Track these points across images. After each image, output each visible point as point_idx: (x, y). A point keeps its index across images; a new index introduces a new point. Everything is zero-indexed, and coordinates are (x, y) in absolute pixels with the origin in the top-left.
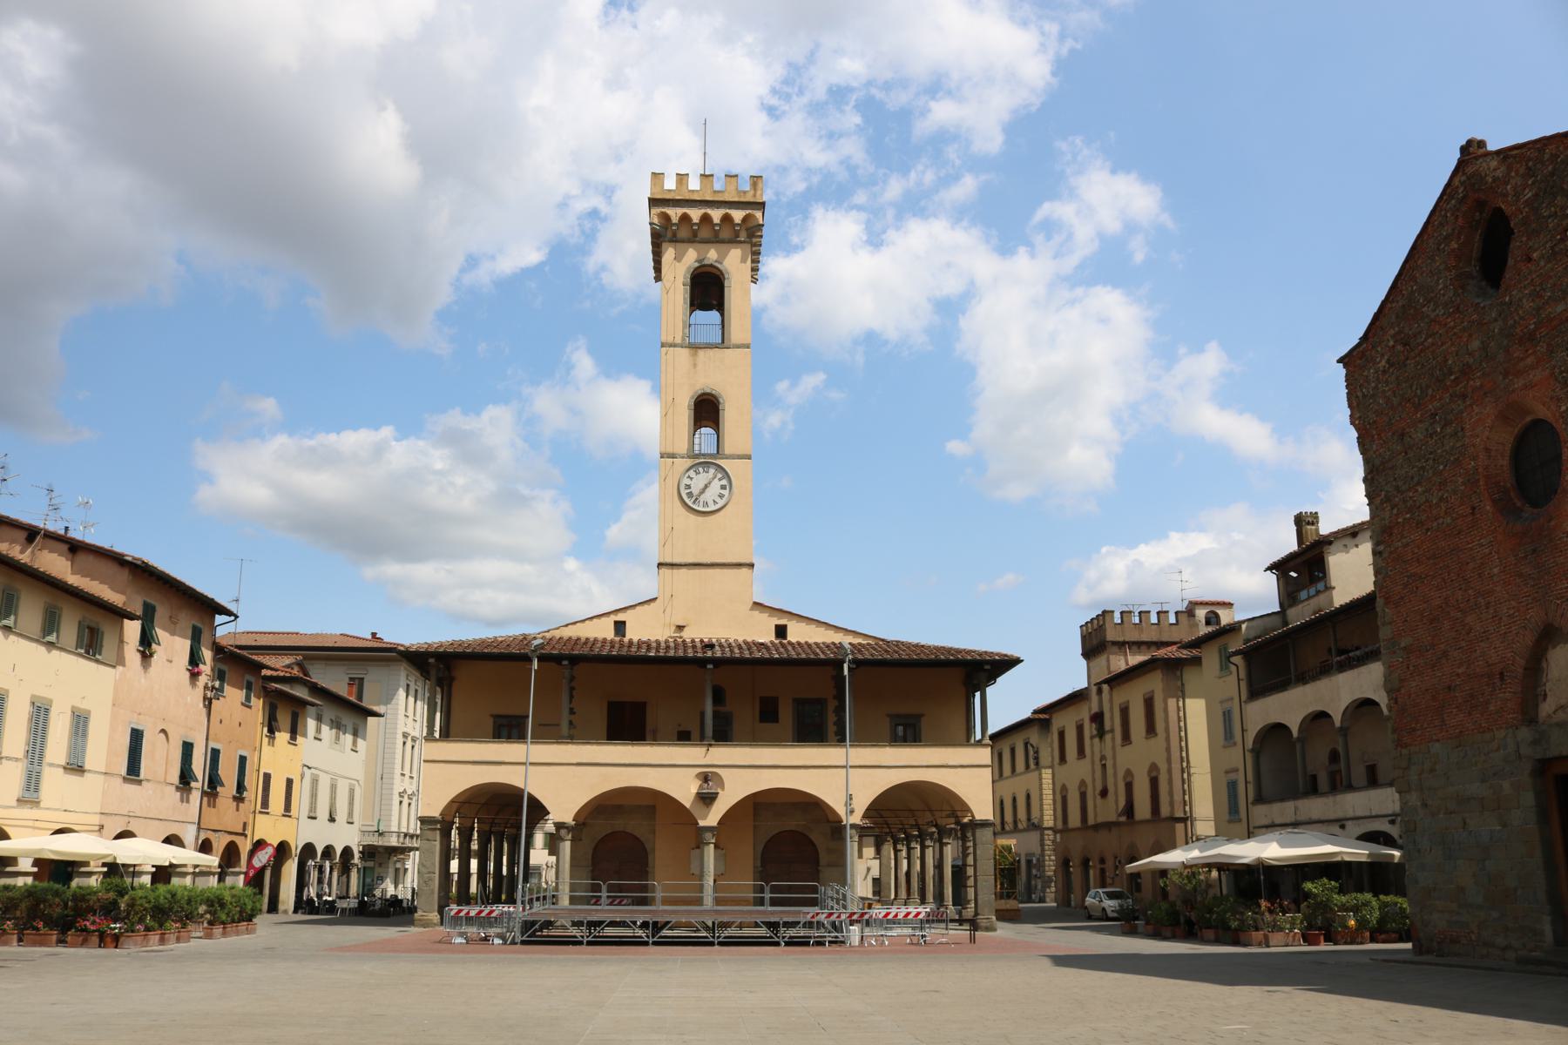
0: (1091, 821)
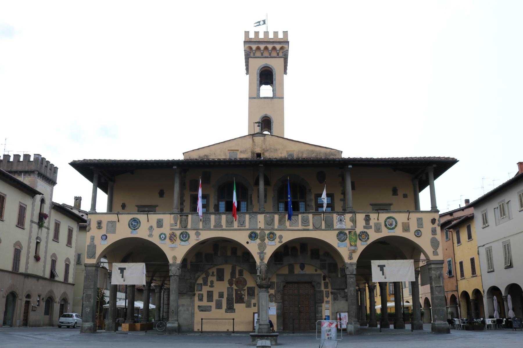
0: (22, 270)
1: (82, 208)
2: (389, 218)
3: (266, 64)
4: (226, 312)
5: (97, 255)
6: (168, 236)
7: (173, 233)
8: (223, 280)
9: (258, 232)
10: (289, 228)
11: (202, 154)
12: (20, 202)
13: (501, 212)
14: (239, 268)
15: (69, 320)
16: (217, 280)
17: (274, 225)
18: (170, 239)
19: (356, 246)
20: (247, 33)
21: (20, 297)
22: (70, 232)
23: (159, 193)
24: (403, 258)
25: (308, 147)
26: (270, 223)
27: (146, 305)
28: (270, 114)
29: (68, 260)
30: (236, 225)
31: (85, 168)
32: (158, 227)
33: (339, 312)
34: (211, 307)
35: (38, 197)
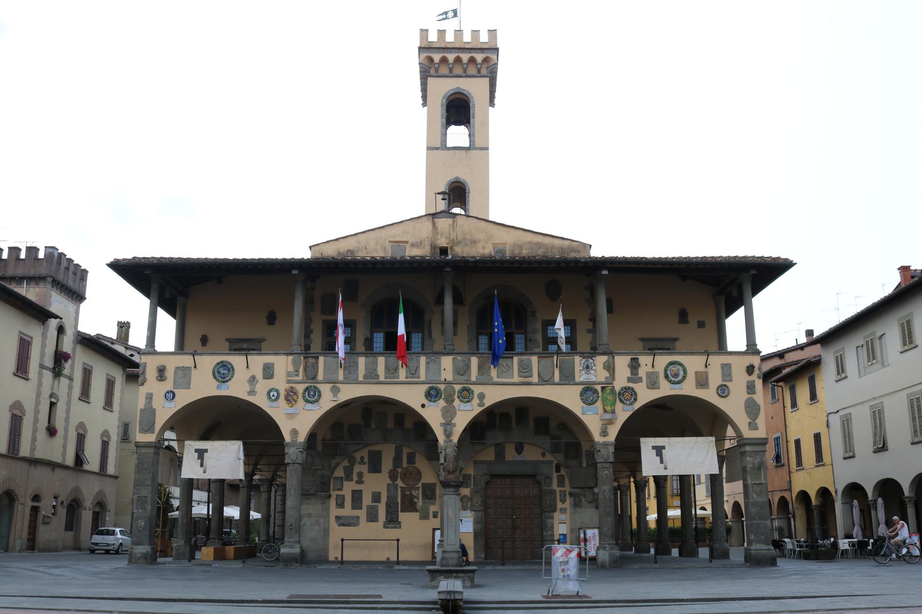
0: (25, 450)
1: (132, 342)
2: (671, 363)
3: (458, 88)
4: (385, 527)
5: (158, 427)
6: (283, 394)
7: (292, 388)
8: (380, 472)
9: (442, 387)
10: (496, 380)
11: (343, 247)
12: (21, 333)
13: (868, 354)
14: (409, 451)
15: (109, 539)
16: (370, 472)
17: (470, 376)
18: (287, 399)
19: (613, 412)
20: (424, 32)
21: (22, 500)
22: (110, 384)
23: (267, 318)
24: (698, 434)
25: (530, 237)
26: (462, 371)
27: (245, 513)
28: (463, 176)
29: (106, 433)
30: (402, 374)
31: (135, 272)
32: (265, 378)
33: (584, 528)
34: (358, 518)
35: (53, 323)
